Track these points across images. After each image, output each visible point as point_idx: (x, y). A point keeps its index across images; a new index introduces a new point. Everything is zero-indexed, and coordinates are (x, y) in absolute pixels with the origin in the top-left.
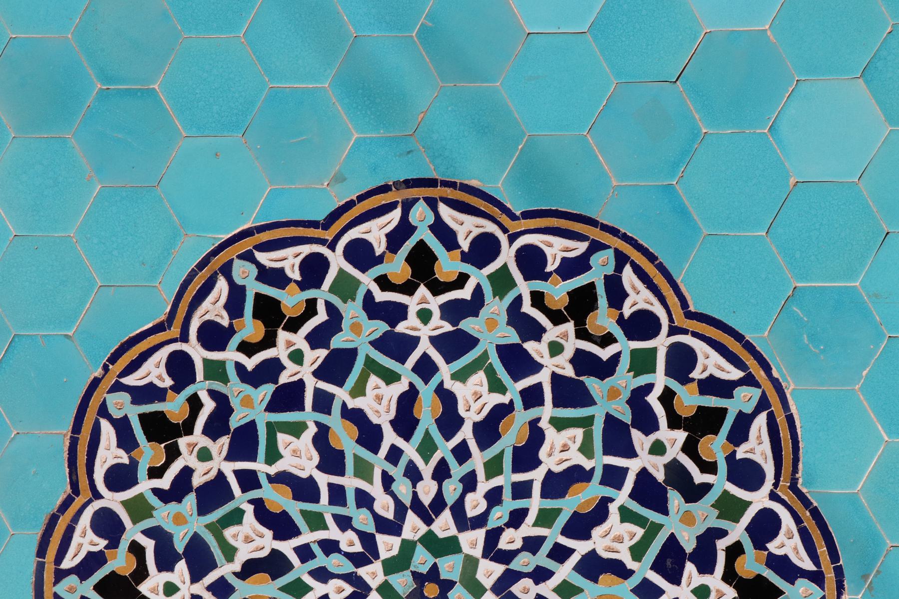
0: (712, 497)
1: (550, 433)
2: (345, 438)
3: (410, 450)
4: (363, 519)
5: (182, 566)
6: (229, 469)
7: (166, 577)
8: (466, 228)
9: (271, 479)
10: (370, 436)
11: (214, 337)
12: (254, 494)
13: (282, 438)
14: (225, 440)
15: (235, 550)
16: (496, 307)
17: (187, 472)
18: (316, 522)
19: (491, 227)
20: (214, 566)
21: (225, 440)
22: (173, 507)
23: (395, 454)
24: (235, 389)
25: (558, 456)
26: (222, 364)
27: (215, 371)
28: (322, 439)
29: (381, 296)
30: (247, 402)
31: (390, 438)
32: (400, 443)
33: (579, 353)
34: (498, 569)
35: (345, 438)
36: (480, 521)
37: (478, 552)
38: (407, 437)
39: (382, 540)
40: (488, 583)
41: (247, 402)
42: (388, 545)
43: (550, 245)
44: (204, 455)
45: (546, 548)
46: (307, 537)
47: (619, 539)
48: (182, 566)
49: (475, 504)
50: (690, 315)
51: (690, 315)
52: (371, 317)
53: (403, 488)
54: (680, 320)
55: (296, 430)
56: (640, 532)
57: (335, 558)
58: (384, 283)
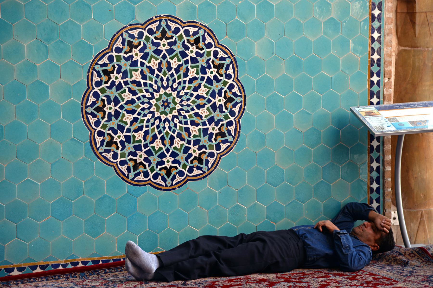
0: (118, 63)
1: (126, 100)
2: (149, 138)
3: (144, 124)
4: (161, 125)
5: (189, 152)
6: (168, 155)
7: (193, 153)
8: (99, 139)
9: (165, 146)
10: (147, 133)
11: (146, 175)
12: (169, 148)
13: (157, 149)
14: (163, 159)
15: (181, 145)
16: (110, 125)
17: (173, 162)
18: (167, 133)
19: (96, 135)
20: (186, 146)
21: (163, 159)
22: (181, 161)
23: (147, 126)
24: (154, 164)
25: (129, 96)
26: (150, 169)
27: (152, 170)
28: (152, 142)
29: (120, 147)
30: (154, 160)
31: (145, 129)
32: (144, 127)
33: (108, 104)
34: (155, 94)
35: (149, 138)
36: (149, 103)
37: (154, 100)
38: (142, 127)
39: (163, 119)
40: (158, 94)
41: (154, 160)
42: (163, 117)
43: (92, 122)
44: (168, 161)
45: (146, 88)
46: (171, 133)
47: (136, 75)
48: (189, 152)
49: (146, 106)
50: (89, 87)
51: (89, 87)
52: (125, 147)
53: (152, 121)
54: (91, 88)
55: (153, 147)
56: (133, 72)
57: (171, 126)
58: (118, 148)
